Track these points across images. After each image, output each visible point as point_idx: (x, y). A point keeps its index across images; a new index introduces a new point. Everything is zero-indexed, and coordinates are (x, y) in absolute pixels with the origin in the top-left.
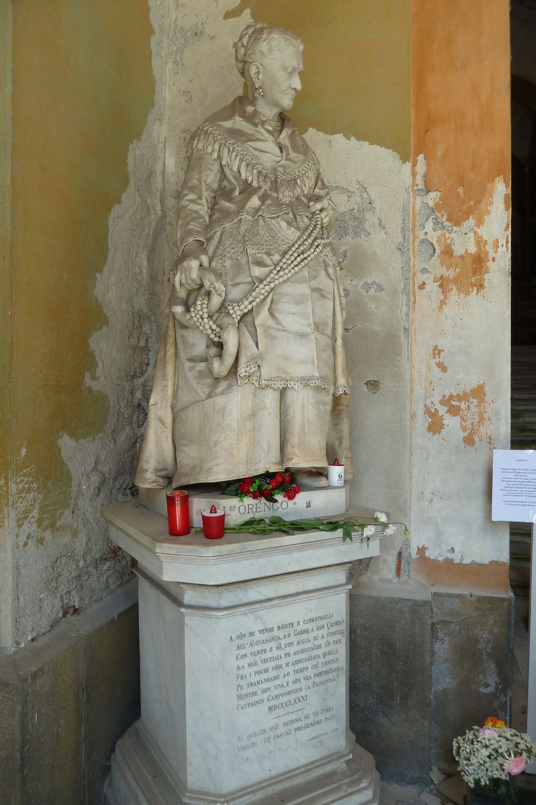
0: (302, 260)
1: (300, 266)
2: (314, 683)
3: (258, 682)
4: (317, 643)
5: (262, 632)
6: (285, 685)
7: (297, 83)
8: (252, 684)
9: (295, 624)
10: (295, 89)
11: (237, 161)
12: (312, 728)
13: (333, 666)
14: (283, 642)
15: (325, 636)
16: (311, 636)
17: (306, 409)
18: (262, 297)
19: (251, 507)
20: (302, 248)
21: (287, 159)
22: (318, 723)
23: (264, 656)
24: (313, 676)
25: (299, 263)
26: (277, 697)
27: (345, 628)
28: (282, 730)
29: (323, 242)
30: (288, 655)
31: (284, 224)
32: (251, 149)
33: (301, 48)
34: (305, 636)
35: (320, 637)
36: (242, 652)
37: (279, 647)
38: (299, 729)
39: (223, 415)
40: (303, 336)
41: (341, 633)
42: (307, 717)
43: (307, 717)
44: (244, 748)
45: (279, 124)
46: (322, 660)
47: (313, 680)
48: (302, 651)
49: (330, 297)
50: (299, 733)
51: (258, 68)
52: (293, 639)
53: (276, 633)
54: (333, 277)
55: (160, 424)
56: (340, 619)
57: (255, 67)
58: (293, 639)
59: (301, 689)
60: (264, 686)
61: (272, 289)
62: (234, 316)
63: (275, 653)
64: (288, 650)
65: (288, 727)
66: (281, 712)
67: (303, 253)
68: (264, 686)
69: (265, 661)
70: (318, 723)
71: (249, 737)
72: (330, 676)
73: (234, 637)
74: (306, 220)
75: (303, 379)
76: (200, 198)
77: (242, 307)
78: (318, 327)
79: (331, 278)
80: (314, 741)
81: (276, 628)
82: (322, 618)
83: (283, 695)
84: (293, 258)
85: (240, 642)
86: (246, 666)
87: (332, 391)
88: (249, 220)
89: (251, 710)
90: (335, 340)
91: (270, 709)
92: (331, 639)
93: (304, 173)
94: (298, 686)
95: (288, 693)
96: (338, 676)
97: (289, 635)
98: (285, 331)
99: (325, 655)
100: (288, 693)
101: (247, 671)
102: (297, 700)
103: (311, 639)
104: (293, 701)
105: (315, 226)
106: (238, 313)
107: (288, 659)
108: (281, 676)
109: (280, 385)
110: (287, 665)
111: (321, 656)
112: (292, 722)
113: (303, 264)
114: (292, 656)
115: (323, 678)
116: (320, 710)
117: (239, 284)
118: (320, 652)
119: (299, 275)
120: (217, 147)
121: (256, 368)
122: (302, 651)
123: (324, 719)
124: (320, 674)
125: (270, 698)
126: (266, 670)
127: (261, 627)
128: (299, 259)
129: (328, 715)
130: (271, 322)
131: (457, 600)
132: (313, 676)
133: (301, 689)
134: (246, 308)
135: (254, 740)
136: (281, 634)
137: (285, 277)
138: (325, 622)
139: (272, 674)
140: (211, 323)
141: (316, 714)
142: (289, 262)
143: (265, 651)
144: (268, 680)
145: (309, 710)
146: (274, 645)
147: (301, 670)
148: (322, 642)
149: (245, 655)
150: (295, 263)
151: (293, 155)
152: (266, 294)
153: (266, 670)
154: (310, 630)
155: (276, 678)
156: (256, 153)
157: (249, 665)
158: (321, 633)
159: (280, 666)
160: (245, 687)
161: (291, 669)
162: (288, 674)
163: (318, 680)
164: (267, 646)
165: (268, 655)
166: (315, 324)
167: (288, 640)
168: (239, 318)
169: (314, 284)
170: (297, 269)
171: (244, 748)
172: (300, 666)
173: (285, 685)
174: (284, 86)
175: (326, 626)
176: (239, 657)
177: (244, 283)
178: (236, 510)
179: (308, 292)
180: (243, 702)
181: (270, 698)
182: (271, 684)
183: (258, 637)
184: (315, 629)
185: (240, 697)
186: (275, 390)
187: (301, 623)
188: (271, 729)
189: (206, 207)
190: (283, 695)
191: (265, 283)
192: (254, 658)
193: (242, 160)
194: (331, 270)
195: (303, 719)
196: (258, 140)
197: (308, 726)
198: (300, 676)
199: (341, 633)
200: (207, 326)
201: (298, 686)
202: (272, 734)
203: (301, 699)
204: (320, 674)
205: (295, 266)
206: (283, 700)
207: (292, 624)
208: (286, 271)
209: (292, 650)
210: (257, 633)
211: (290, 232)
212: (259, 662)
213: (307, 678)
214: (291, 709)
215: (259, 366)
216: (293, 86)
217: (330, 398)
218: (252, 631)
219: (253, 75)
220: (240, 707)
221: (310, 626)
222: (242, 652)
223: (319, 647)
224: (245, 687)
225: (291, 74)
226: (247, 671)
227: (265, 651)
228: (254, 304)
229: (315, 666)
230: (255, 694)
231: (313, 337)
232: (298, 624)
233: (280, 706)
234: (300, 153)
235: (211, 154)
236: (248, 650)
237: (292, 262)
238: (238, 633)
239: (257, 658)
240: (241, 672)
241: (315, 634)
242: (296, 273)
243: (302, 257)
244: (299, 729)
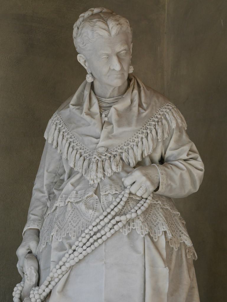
0: (95, 241)
18: (57, 280)
20: (95, 229)
21: (108, 137)
25: (92, 244)
29: (123, 218)
33: (114, 32)
67: (95, 234)
74: (110, 198)
79: (136, 251)
84: (84, 241)
88: (62, 206)
93: (135, 144)
113: (96, 244)
128: (91, 240)
137: (76, 260)
142: (81, 244)
150: (88, 244)
151: (117, 131)
170: (89, 250)
189: (46, 194)
208: (76, 253)
216: (112, 68)
219: (83, 64)
228: (50, 287)
235: (52, 144)
237: (84, 244)
243: (95, 237)
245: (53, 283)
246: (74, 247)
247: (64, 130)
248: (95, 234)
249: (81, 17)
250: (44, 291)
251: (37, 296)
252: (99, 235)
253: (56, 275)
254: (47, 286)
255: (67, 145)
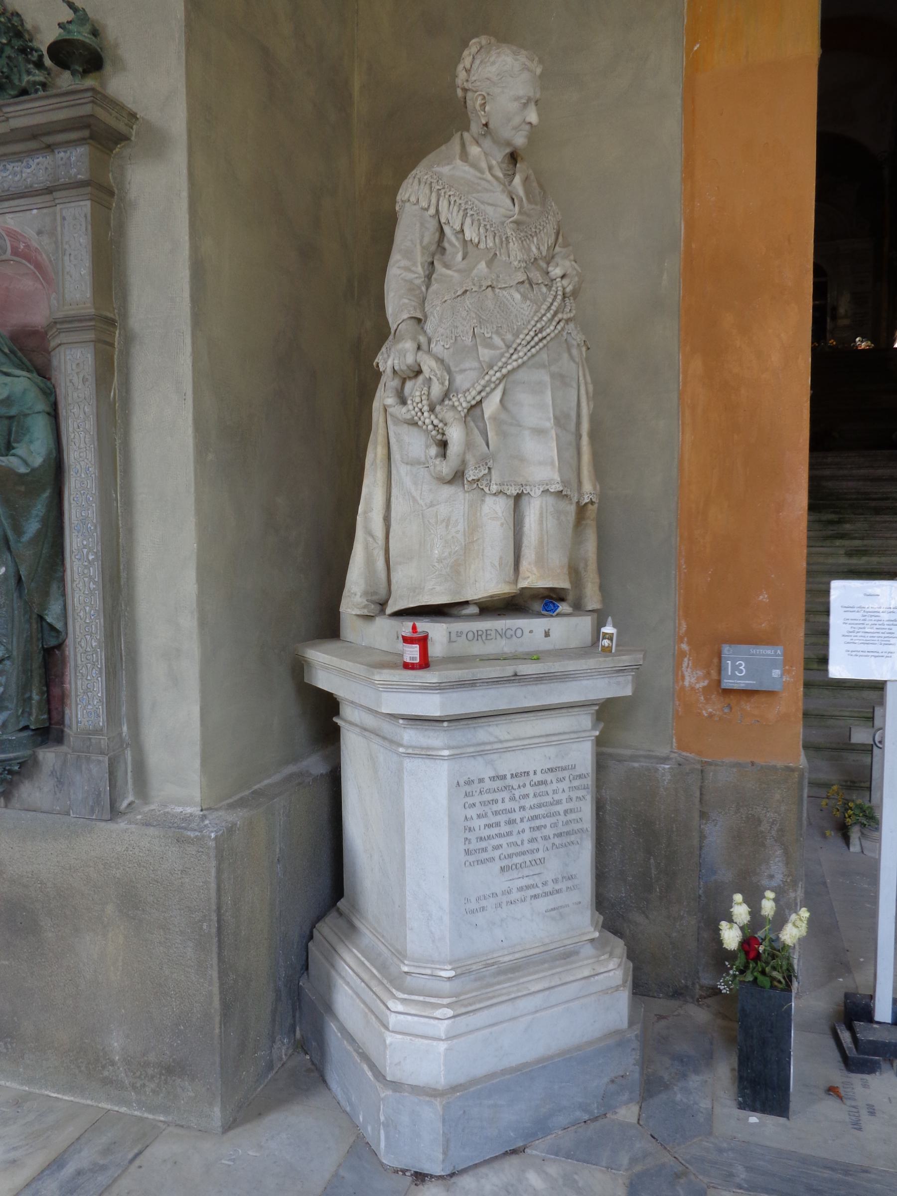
0: (541, 340)
1: (537, 347)
2: (553, 844)
3: (489, 837)
4: (557, 797)
5: (492, 779)
6: (519, 843)
7: (533, 117)
8: (481, 839)
9: (532, 773)
10: (530, 123)
11: (460, 217)
12: (550, 897)
13: (576, 826)
14: (517, 793)
15: (566, 789)
16: (549, 788)
17: (544, 519)
18: (493, 386)
19: (480, 633)
20: (539, 326)
22: (558, 892)
23: (495, 807)
24: (552, 836)
25: (537, 344)
26: (510, 856)
27: (590, 783)
28: (516, 895)
30: (522, 808)
31: (517, 296)
32: (476, 202)
34: (543, 788)
35: (561, 790)
36: (470, 800)
37: (512, 799)
38: (535, 897)
39: (447, 526)
40: (539, 432)
41: (585, 788)
42: (545, 884)
43: (545, 884)
44: (473, 912)
45: (511, 166)
46: (562, 818)
47: (552, 841)
48: (540, 806)
49: (575, 385)
50: (536, 902)
51: (484, 98)
52: (529, 790)
53: (509, 781)
54: (577, 360)
55: (371, 539)
56: (584, 772)
57: (480, 98)
58: (529, 790)
59: (538, 850)
60: (495, 842)
61: (504, 376)
62: (460, 409)
63: (508, 805)
64: (523, 802)
65: (523, 893)
66: (515, 874)
68: (495, 842)
69: (496, 813)
70: (558, 892)
71: (478, 899)
72: (573, 838)
73: (462, 783)
74: (544, 289)
75: (541, 483)
76: (415, 264)
77: (469, 398)
78: (559, 421)
79: (574, 361)
80: (553, 913)
81: (509, 776)
82: (564, 769)
83: (518, 854)
84: (528, 338)
85: (468, 789)
86: (475, 817)
87: (575, 500)
89: (481, 868)
90: (579, 437)
91: (502, 869)
92: (574, 795)
94: (535, 846)
95: (523, 853)
96: (581, 839)
97: (524, 786)
98: (520, 426)
99: (566, 812)
100: (523, 853)
101: (477, 823)
102: (533, 863)
103: (550, 792)
104: (528, 863)
105: (555, 297)
106: (464, 405)
107: (523, 814)
108: (515, 833)
109: (513, 491)
110: (522, 820)
111: (562, 813)
112: (528, 887)
113: (541, 345)
114: (527, 810)
115: (565, 840)
116: (560, 877)
117: (465, 370)
118: (560, 808)
119: (536, 359)
120: (434, 201)
121: (486, 471)
122: (540, 806)
123: (564, 888)
124: (560, 835)
125: (502, 857)
126: (498, 824)
127: (492, 774)
128: (536, 339)
129: (570, 884)
130: (504, 416)
131: (735, 770)
132: (552, 836)
133: (538, 850)
134: (474, 398)
135: (484, 903)
136: (515, 783)
137: (520, 361)
138: (566, 774)
139: (504, 829)
140: (433, 417)
141: (555, 881)
142: (524, 342)
143: (496, 801)
144: (499, 835)
145: (549, 876)
146: (506, 795)
147: (538, 828)
148: (564, 797)
149: (474, 805)
150: (532, 343)
152: (497, 382)
153: (498, 824)
154: (549, 782)
155: (509, 834)
156: (482, 207)
157: (479, 816)
158: (561, 786)
159: (514, 821)
160: (474, 841)
161: (526, 825)
162: (523, 831)
163: (557, 841)
164: (498, 796)
165: (500, 806)
166: (555, 418)
167: (524, 791)
168: (466, 411)
169: (554, 368)
170: (533, 350)
171: (473, 912)
172: (538, 823)
173: (519, 843)
174: (517, 120)
175: (567, 779)
176: (467, 805)
177: (470, 369)
178: (464, 636)
179: (547, 379)
180: (471, 858)
181: (502, 857)
182: (503, 841)
183: (488, 784)
184: (554, 781)
185: (468, 852)
186: (508, 496)
187: (538, 772)
188: (503, 893)
190: (517, 854)
191: (496, 368)
192: (484, 808)
193: (465, 216)
194: (575, 352)
195: (540, 885)
196: (487, 190)
197: (546, 894)
198: (537, 834)
199: (585, 788)
200: (427, 421)
201: (535, 846)
202: (505, 899)
203: (538, 862)
204: (560, 835)
205: (532, 347)
206: (517, 860)
207: (528, 773)
208: (521, 354)
209: (527, 803)
210: (487, 780)
211: (525, 306)
212: (490, 814)
213: (545, 838)
214: (526, 872)
215: (489, 468)
216: (528, 119)
217: (572, 509)
218: (481, 777)
219: (478, 107)
220: (467, 864)
221: (549, 777)
222: (470, 800)
223: (559, 802)
224: (474, 841)
225: (525, 105)
226: (477, 823)
227: (496, 801)
228: (483, 394)
229: (555, 825)
230: (485, 850)
231: (553, 433)
232: (535, 773)
233: (514, 867)
234: (536, 204)
236: (476, 799)
237: (529, 343)
238: (466, 778)
239: (487, 809)
240: (468, 824)
241: (555, 786)
242: (533, 356)
243: (540, 336)
244: (535, 897)
245: (488, 389)
246: (514, 346)
247: (451, 193)
248: (541, 330)
249: (475, 43)
250: (474, 398)
251: (464, 405)
252: (544, 334)
253: (494, 379)
254: (480, 393)
255: (461, 213)
